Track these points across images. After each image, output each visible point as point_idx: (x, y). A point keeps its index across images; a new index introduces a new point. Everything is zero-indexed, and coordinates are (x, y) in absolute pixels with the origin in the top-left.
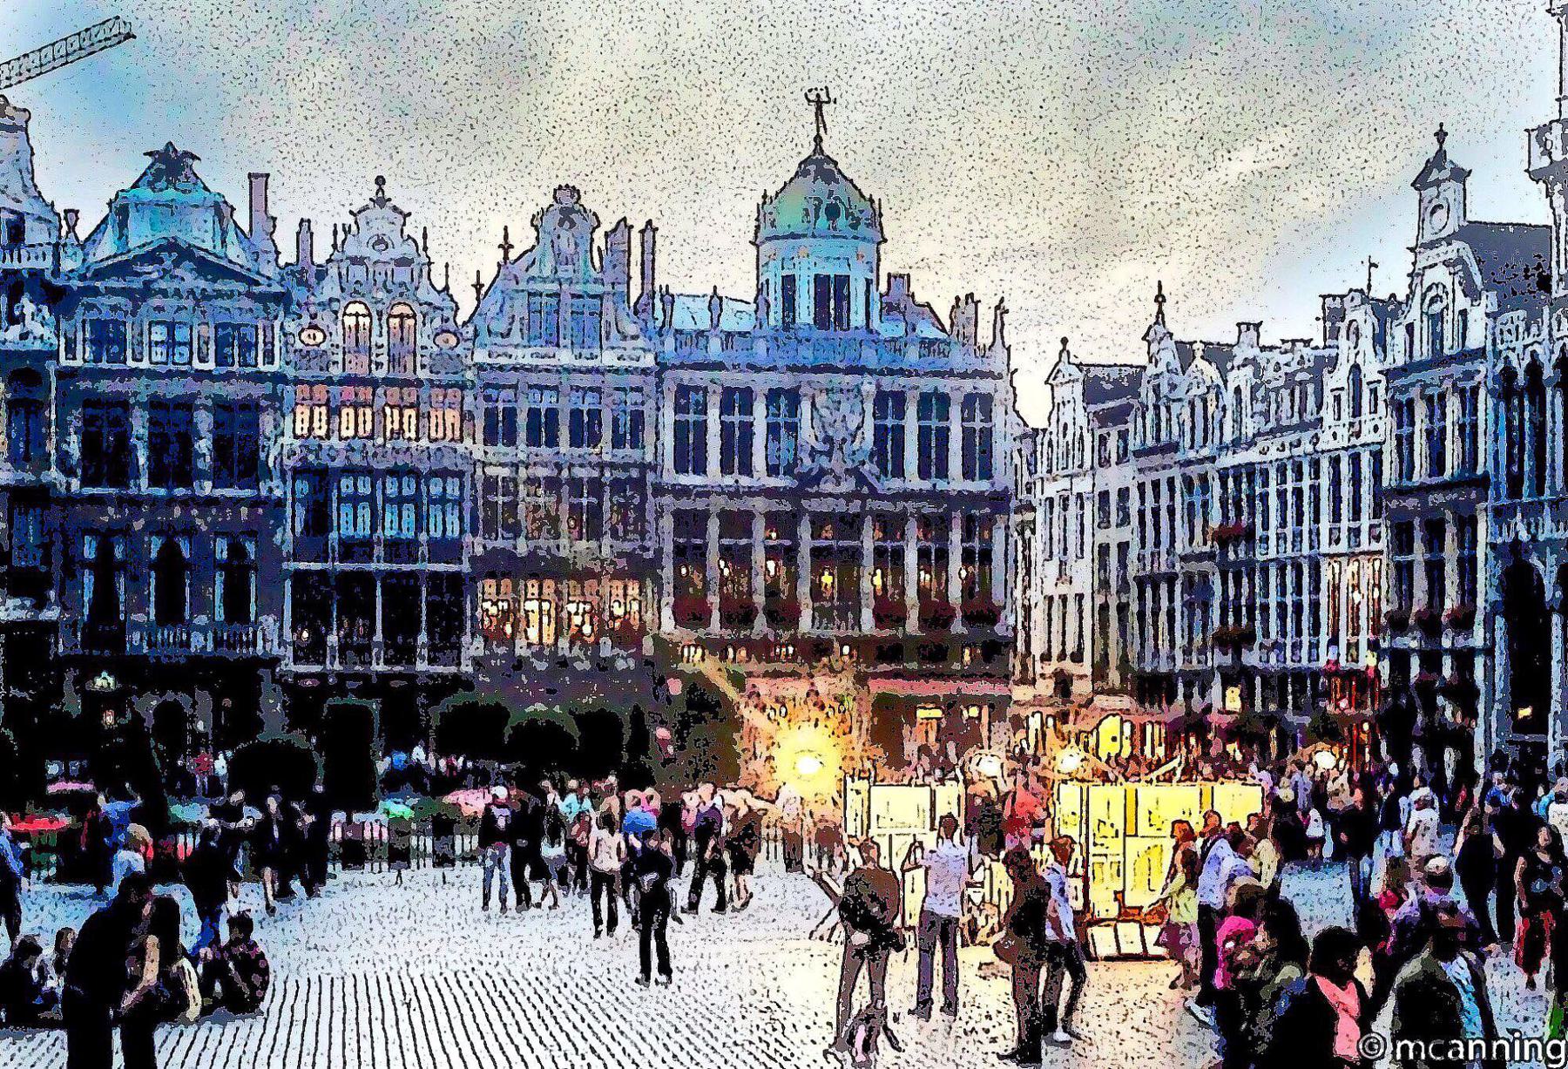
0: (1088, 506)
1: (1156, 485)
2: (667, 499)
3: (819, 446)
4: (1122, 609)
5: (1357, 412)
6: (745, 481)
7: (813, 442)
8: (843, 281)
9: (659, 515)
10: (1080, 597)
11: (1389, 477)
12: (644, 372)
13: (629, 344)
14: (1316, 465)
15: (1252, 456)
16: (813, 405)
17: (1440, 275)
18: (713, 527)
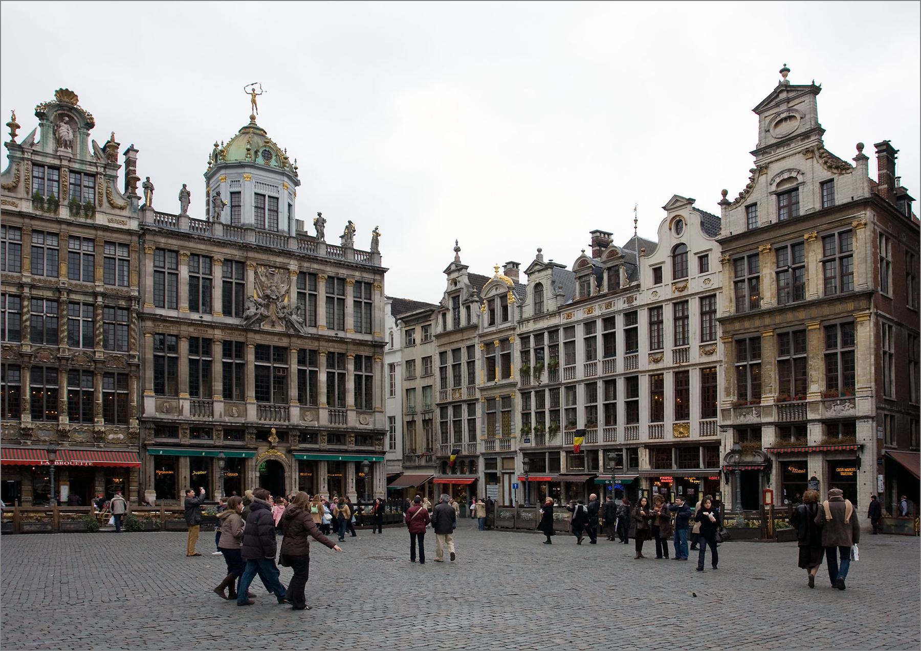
5: (680, 270)
6: (207, 318)
14: (631, 316)
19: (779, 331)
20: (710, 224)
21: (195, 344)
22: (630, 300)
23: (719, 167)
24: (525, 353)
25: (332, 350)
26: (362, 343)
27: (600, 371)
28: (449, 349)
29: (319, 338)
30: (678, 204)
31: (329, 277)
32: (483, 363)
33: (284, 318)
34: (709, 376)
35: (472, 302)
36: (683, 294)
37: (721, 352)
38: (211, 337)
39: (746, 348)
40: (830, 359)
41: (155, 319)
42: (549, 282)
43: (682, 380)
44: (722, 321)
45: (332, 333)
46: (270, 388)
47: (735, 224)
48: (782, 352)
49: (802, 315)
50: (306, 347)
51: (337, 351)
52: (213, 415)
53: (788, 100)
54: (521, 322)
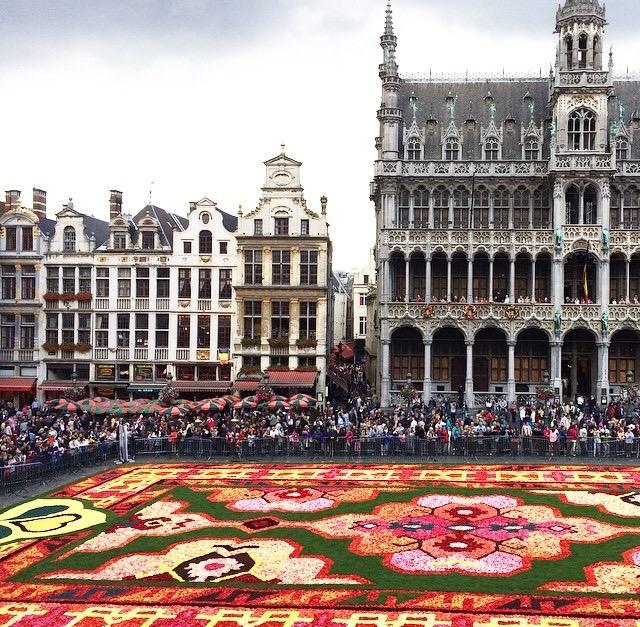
15: (95, 261)
17: (290, 203)
20: (230, 223)
22: (163, 260)
23: (241, 191)
24: (52, 283)
27: (133, 306)
30: (206, 203)
34: (225, 321)
36: (208, 264)
37: (234, 307)
39: (251, 308)
40: (303, 323)
42: (82, 228)
44: (236, 288)
47: (246, 228)
48: (274, 313)
53: (285, 165)
54: (49, 254)
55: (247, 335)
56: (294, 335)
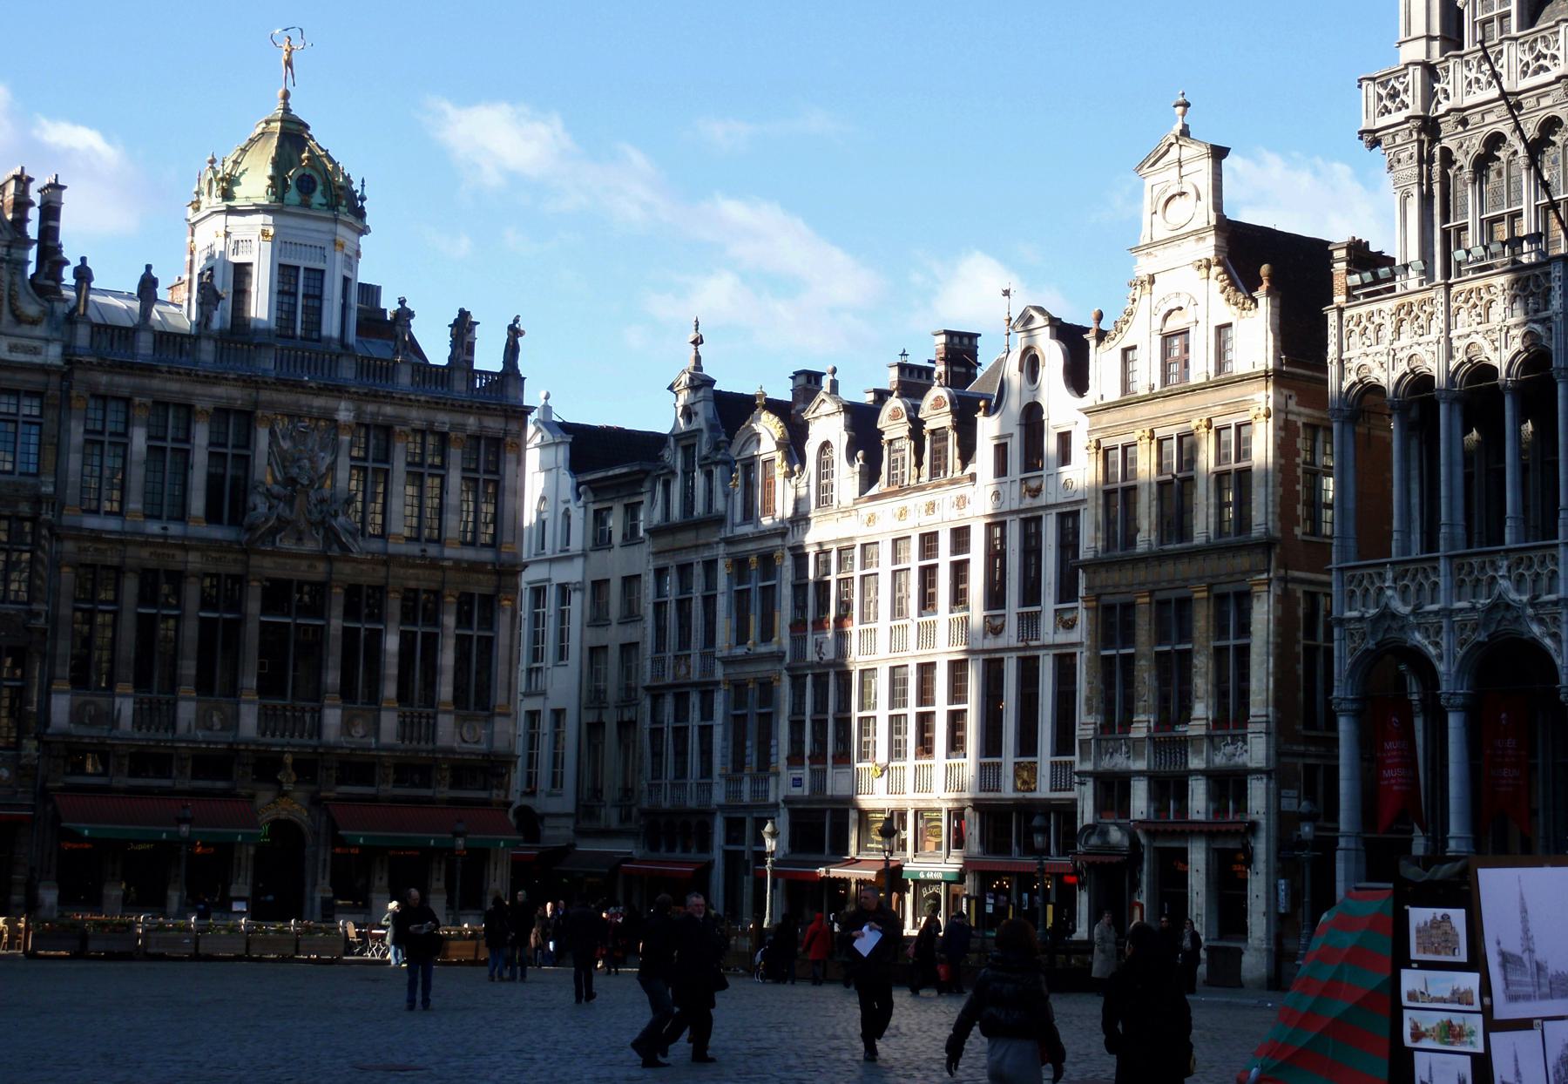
0: (576, 598)
1: (684, 570)
2: (69, 546)
3: (276, 489)
4: (626, 727)
6: (175, 529)
7: (269, 478)
8: (317, 276)
9: (56, 565)
10: (558, 714)
11: (1089, 541)
12: (44, 369)
13: (26, 329)
14: (960, 537)
16: (272, 433)
18: (131, 585)
19: (1160, 596)
21: (150, 581)
25: (412, 584)
26: (475, 567)
28: (671, 562)
29: (388, 560)
31: (415, 431)
32: (729, 603)
33: (323, 522)
34: (1065, 665)
35: (717, 463)
38: (180, 567)
39: (1114, 623)
40: (1220, 653)
41: (79, 534)
43: (1029, 668)
44: (1086, 565)
45: (414, 549)
46: (288, 668)
49: (1184, 569)
50: (362, 580)
51: (423, 585)
52: (174, 729)
55: (1108, 711)
56: (1201, 710)
